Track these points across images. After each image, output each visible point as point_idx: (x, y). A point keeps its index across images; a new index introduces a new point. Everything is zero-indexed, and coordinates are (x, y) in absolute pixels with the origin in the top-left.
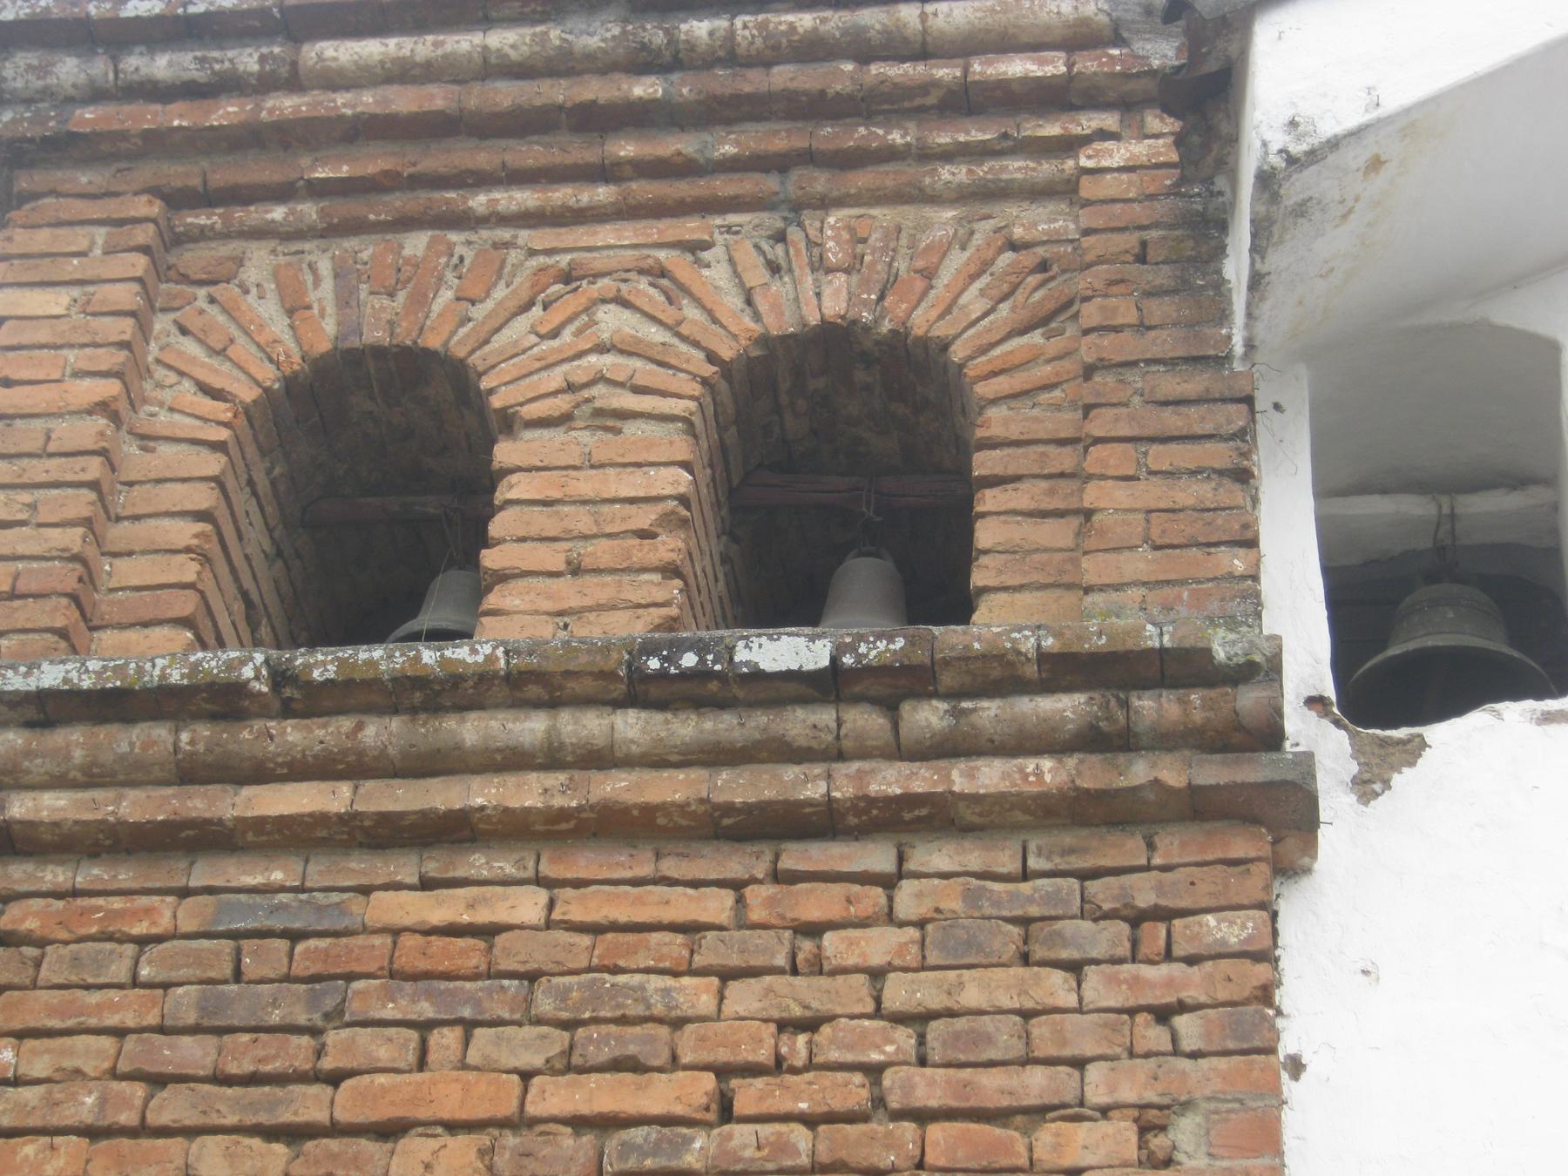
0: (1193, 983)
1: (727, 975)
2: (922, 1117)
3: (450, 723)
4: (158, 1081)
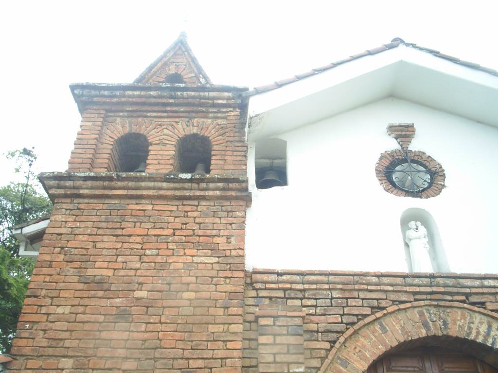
0: (235, 220)
1: (175, 217)
2: (200, 236)
3: (141, 183)
4: (99, 228)
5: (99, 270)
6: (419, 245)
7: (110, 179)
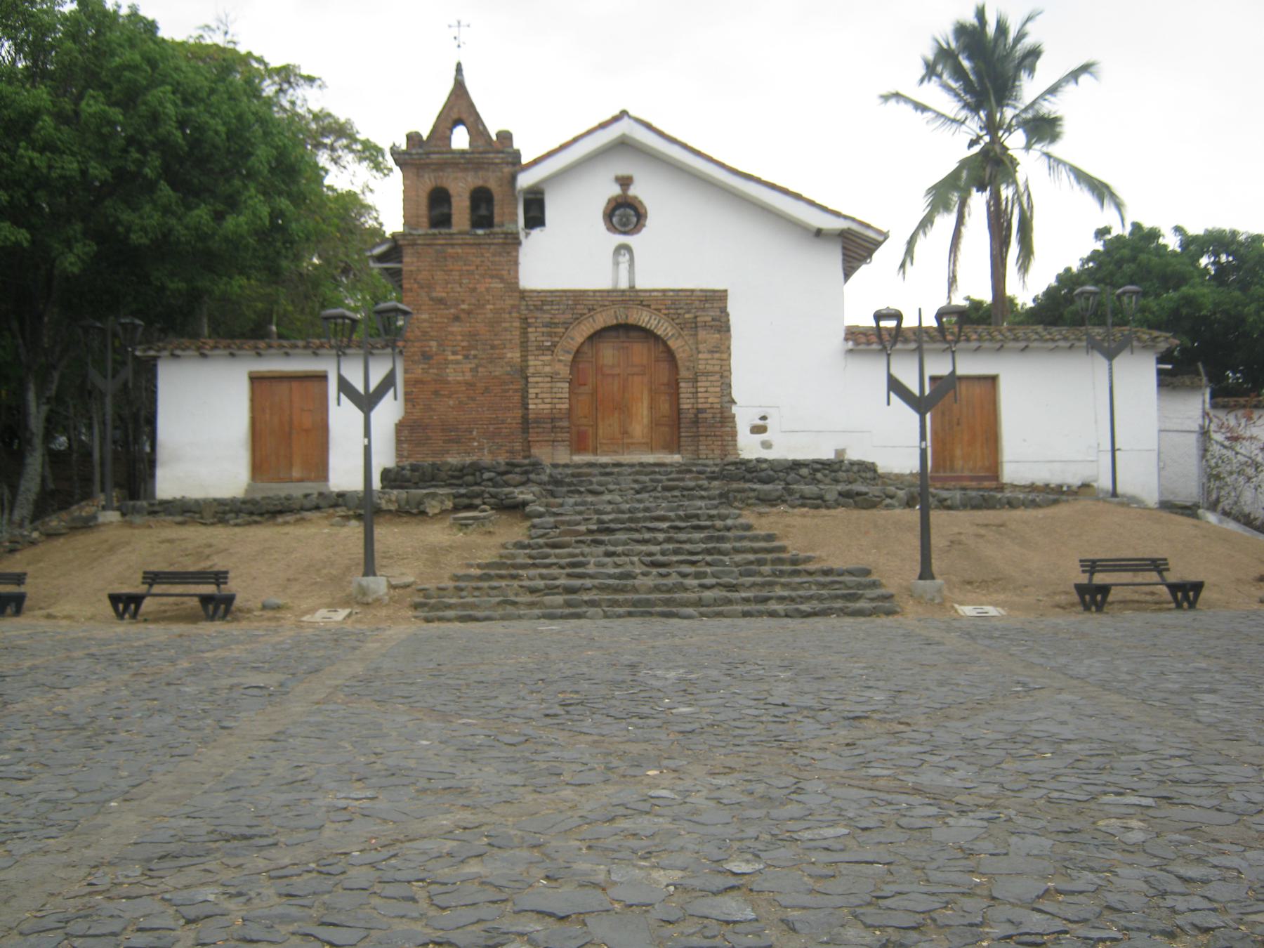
5: (439, 293)
6: (624, 267)
7: (434, 234)
